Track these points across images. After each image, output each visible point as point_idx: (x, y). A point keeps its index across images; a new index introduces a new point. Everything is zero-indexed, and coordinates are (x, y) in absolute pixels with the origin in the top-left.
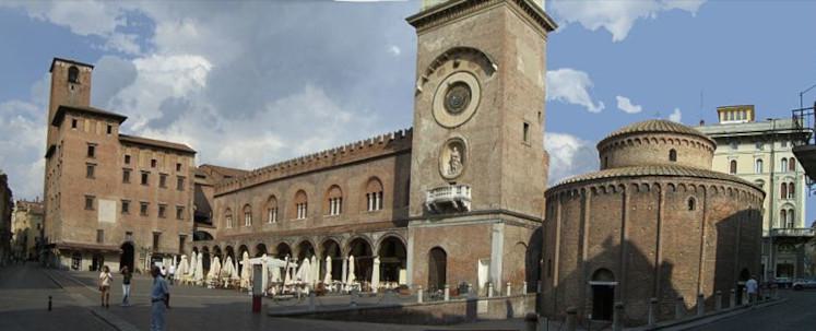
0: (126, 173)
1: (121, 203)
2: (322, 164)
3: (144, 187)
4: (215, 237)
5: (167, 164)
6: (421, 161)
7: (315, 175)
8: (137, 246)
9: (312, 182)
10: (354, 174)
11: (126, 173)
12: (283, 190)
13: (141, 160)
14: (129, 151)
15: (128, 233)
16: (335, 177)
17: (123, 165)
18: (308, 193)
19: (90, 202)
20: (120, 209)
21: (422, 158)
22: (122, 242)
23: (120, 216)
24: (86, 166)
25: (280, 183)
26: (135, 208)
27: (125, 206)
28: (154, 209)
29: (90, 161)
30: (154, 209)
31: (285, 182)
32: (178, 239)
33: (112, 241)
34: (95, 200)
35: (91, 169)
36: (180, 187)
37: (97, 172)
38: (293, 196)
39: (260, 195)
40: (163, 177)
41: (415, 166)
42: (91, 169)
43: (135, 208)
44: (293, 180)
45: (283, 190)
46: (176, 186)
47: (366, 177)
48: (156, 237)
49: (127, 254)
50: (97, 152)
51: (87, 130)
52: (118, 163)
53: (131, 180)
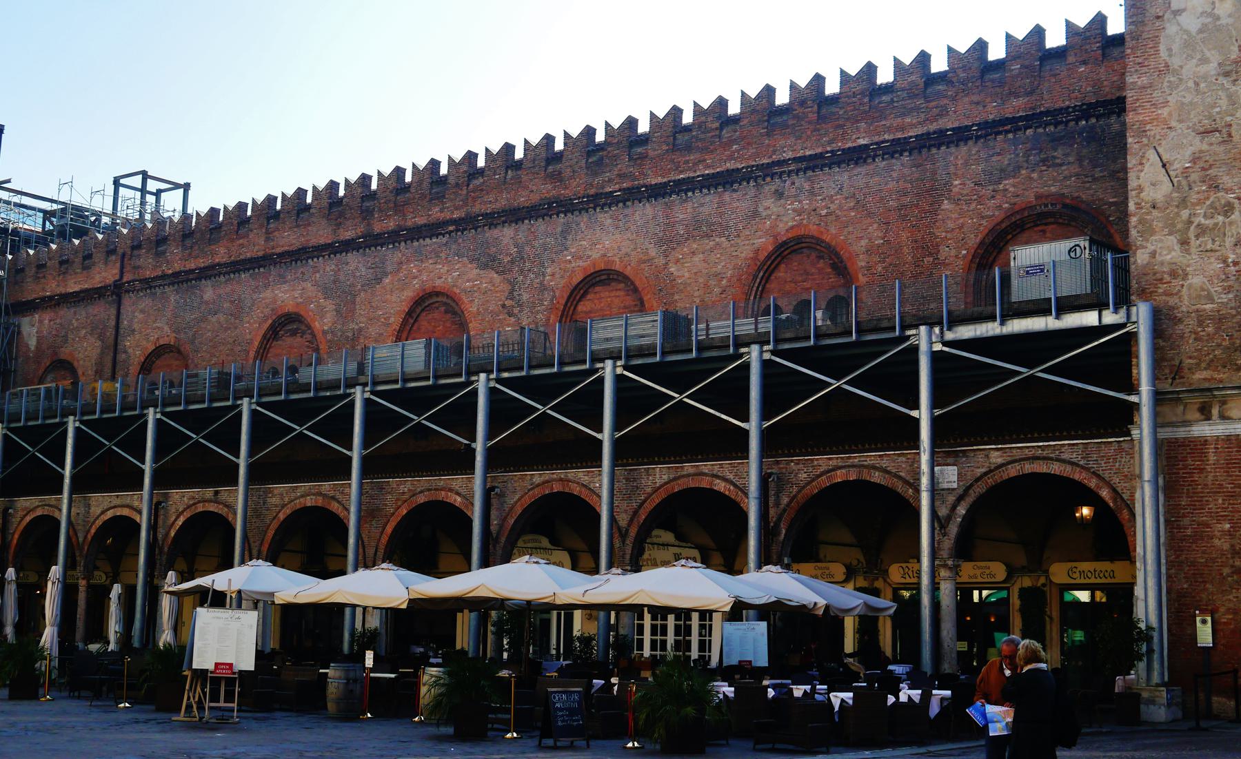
2: (538, 190)
6: (1180, 160)
7: (506, 235)
9: (489, 262)
10: (701, 229)
18: (472, 307)
21: (1181, 146)
25: (327, 267)
31: (355, 263)
41: (1148, 181)
44: (392, 255)
47: (760, 241)
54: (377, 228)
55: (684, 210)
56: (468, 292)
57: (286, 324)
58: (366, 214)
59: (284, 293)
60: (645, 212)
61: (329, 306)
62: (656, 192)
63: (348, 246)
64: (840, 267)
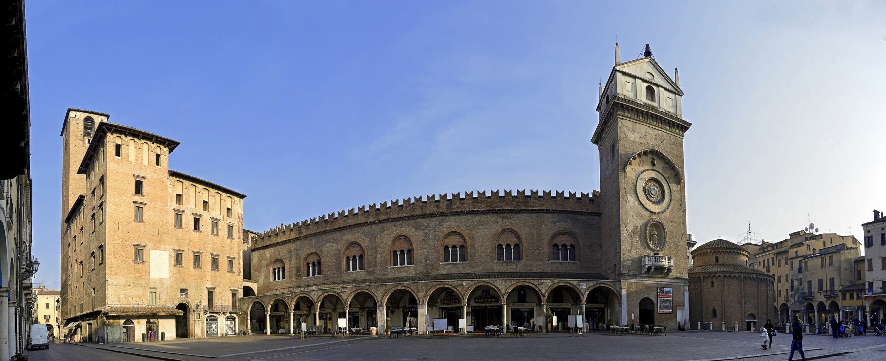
0: (179, 215)
1: (173, 254)
3: (195, 235)
4: (256, 292)
5: (219, 202)
7: (423, 221)
8: (192, 305)
11: (179, 215)
12: (373, 237)
13: (194, 196)
14: (179, 187)
15: (182, 291)
16: (452, 223)
17: (175, 205)
18: (413, 240)
19: (139, 250)
20: (173, 260)
22: (177, 303)
23: (175, 269)
24: (133, 206)
25: (366, 229)
26: (188, 258)
27: (178, 257)
28: (206, 260)
29: (138, 199)
30: (206, 260)
31: (375, 228)
32: (230, 295)
33: (168, 301)
34: (145, 250)
35: (139, 207)
36: (231, 236)
37: (147, 213)
38: (389, 243)
39: (336, 241)
40: (215, 222)
42: (139, 207)
43: (188, 258)
44: (386, 226)
45: (373, 237)
46: (227, 235)
48: (210, 293)
49: (182, 315)
50: (145, 188)
51: (132, 158)
52: (169, 203)
53: (184, 225)
54: (381, 218)
55: (476, 218)
56: (413, 235)
57: (355, 244)
58: (377, 215)
59: (351, 237)
60: (463, 218)
61: (367, 239)
62: (468, 213)
63: (372, 223)
64: (518, 237)
